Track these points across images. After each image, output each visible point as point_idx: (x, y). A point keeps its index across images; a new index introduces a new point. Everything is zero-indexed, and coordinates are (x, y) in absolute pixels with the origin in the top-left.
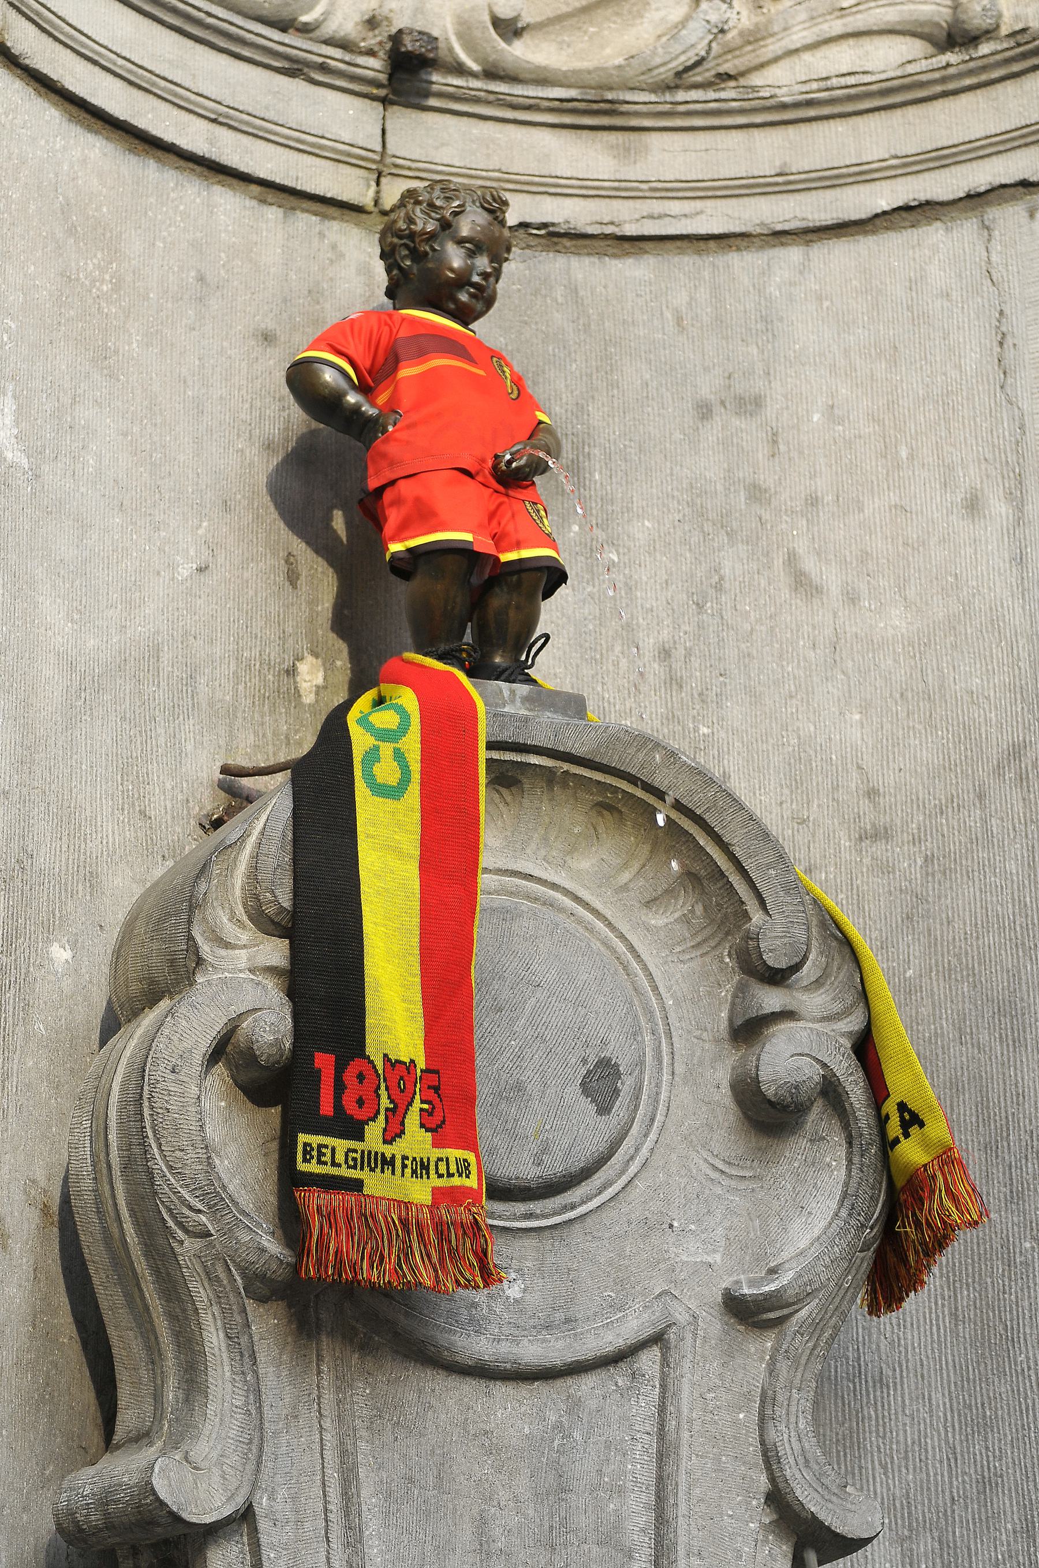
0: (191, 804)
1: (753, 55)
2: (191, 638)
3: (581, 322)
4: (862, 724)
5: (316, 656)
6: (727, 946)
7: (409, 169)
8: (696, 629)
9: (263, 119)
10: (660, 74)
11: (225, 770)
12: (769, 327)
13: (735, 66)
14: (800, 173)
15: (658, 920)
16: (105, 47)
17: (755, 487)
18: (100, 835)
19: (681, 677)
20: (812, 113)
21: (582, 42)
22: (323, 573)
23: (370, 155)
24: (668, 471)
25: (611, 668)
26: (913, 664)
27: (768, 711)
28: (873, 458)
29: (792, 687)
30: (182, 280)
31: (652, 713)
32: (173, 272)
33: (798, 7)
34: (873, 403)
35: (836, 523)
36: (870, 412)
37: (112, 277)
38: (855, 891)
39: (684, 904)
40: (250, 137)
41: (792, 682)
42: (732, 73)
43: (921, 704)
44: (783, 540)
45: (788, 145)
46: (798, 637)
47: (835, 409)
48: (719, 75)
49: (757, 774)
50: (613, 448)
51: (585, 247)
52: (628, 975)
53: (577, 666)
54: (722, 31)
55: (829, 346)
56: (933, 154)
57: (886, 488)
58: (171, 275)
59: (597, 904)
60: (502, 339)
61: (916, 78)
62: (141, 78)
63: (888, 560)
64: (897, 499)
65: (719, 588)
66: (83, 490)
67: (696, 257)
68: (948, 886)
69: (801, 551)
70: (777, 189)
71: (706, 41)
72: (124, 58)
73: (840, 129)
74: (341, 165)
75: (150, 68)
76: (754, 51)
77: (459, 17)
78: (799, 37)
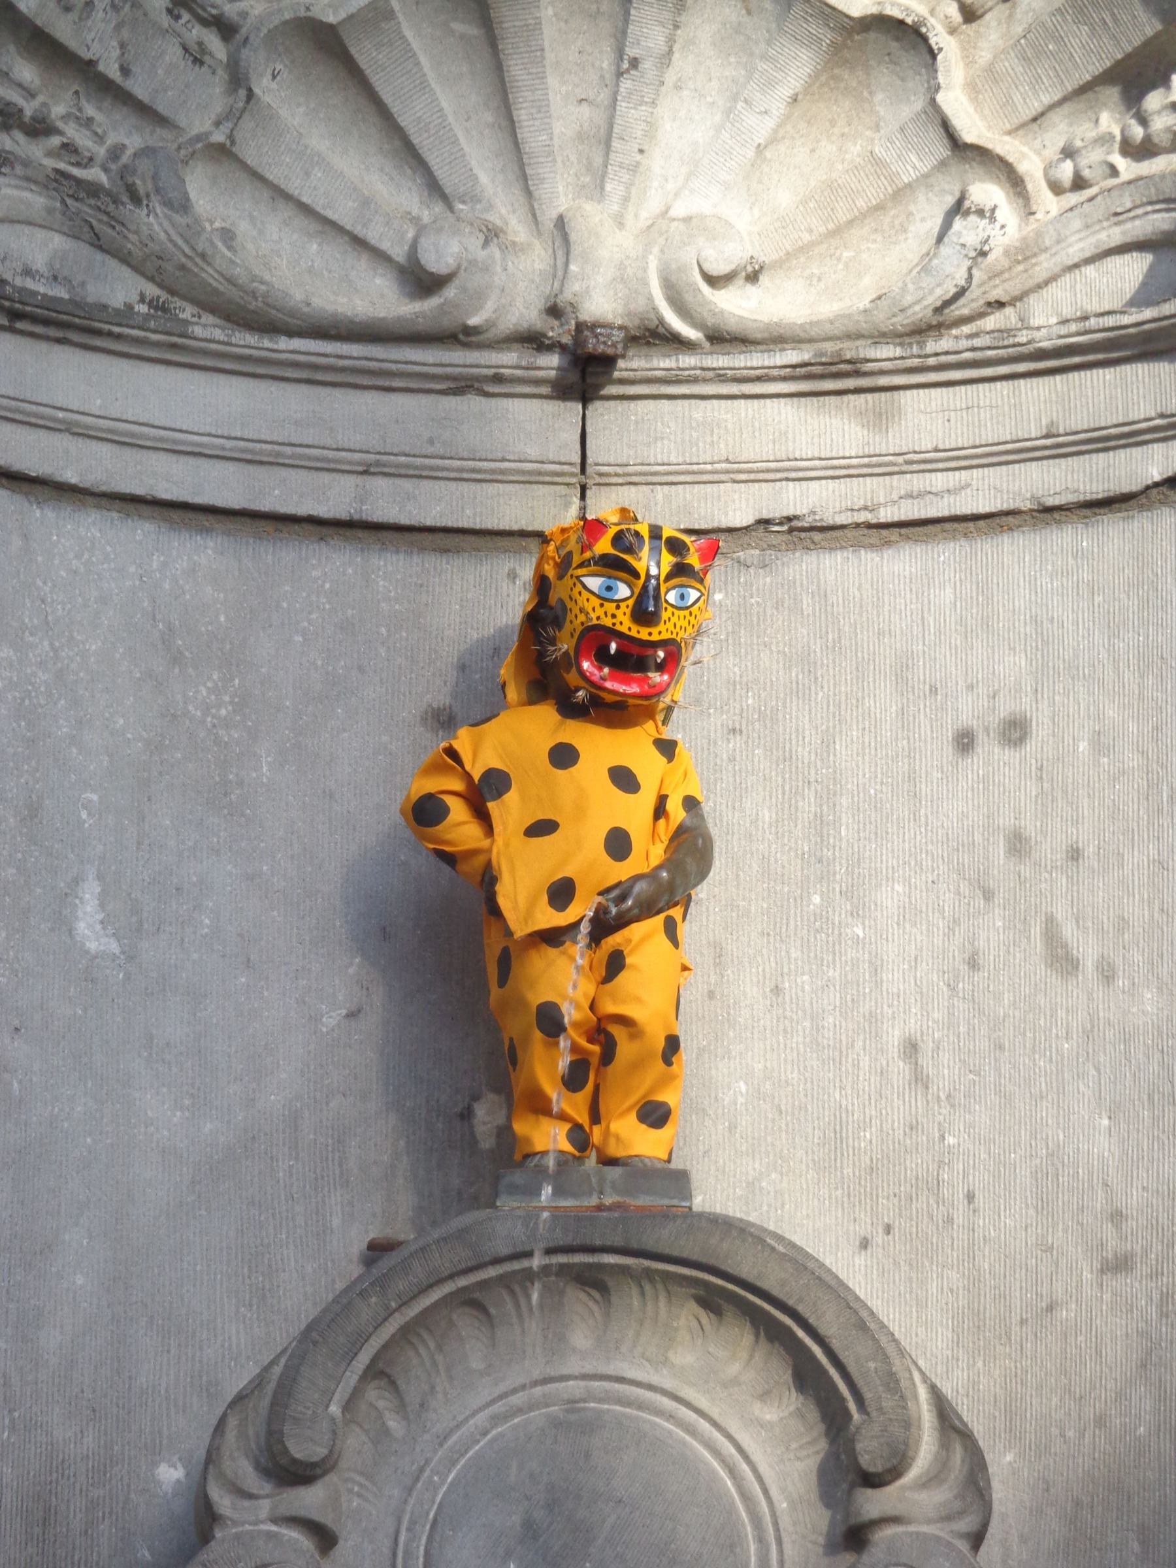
7: (617, 475)
9: (426, 457)
13: (1005, 291)
14: (1067, 434)
16: (209, 435)
18: (220, 1338)
19: (928, 1076)
23: (566, 468)
30: (327, 673)
33: (1069, 214)
40: (414, 480)
42: (1004, 300)
48: (989, 304)
54: (983, 254)
59: (703, 1403)
60: (736, 669)
62: (261, 452)
66: (195, 956)
76: (1026, 271)
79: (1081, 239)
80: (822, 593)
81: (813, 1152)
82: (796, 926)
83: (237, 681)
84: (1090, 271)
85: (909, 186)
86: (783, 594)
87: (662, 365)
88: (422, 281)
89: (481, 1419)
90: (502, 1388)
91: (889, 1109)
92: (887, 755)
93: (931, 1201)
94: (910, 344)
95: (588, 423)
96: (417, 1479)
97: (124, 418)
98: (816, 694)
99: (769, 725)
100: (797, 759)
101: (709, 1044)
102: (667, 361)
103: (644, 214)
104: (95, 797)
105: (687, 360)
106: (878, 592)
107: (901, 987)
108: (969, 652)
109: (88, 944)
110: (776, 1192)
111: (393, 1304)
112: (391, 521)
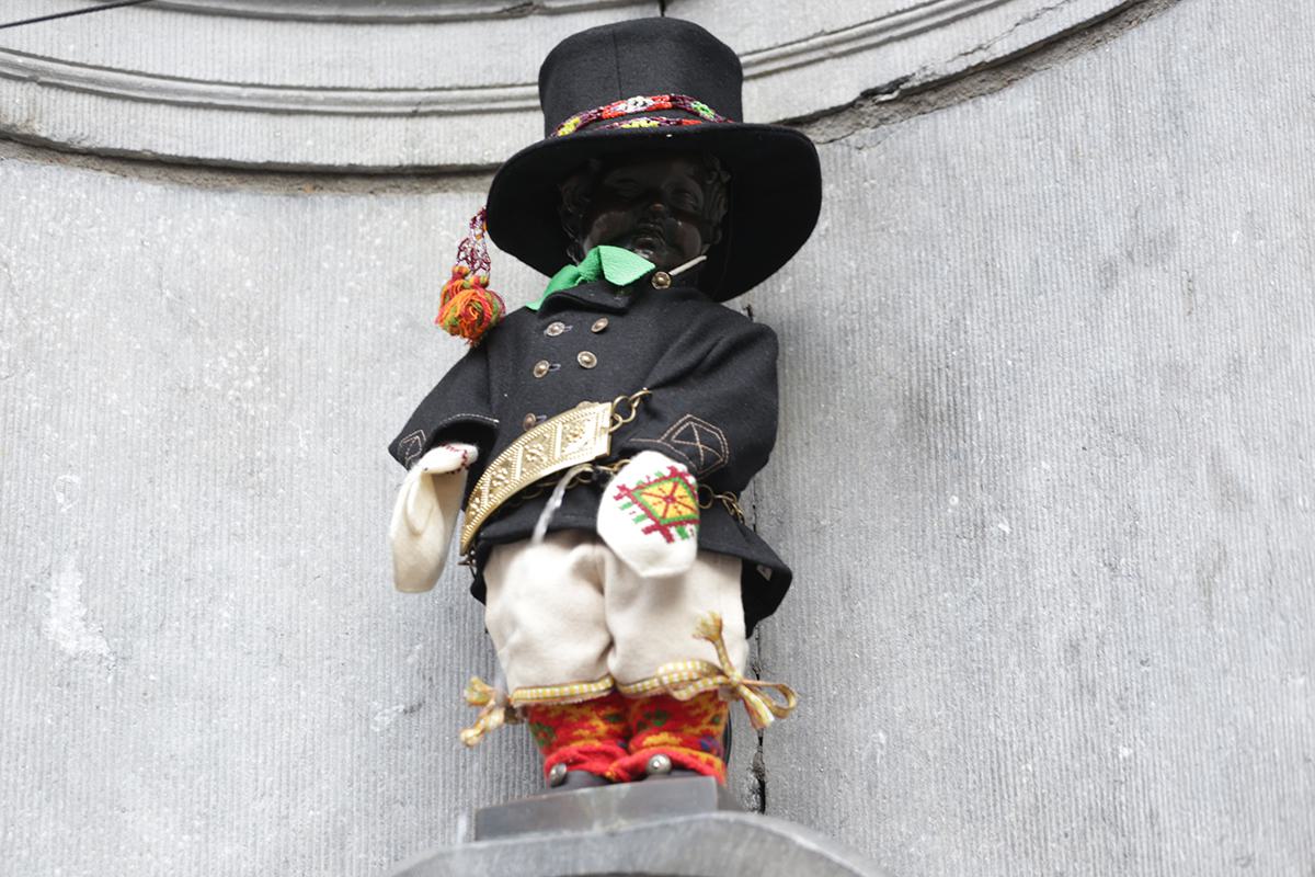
3: (953, 202)
4: (1306, 689)
9: (483, 87)
12: (1179, 123)
16: (220, 83)
24: (1068, 379)
29: (1226, 659)
31: (1058, 744)
32: (366, 330)
37: (262, 367)
40: (474, 117)
41: (1224, 649)
44: (1205, 436)
46: (1227, 578)
47: (1255, 215)
50: (998, 369)
51: (954, 94)
60: (852, 264)
62: (286, 99)
65: (1134, 533)
66: (209, 655)
69: (1226, 445)
72: (253, 85)
75: (294, 84)
80: (942, 156)
81: (968, 802)
82: (934, 536)
83: (266, 350)
86: (900, 168)
91: (1052, 731)
93: (1108, 835)
97: (107, 65)
98: (942, 269)
101: (840, 693)
104: (76, 479)
107: (1057, 582)
109: (63, 644)
110: (927, 856)
112: (449, 162)
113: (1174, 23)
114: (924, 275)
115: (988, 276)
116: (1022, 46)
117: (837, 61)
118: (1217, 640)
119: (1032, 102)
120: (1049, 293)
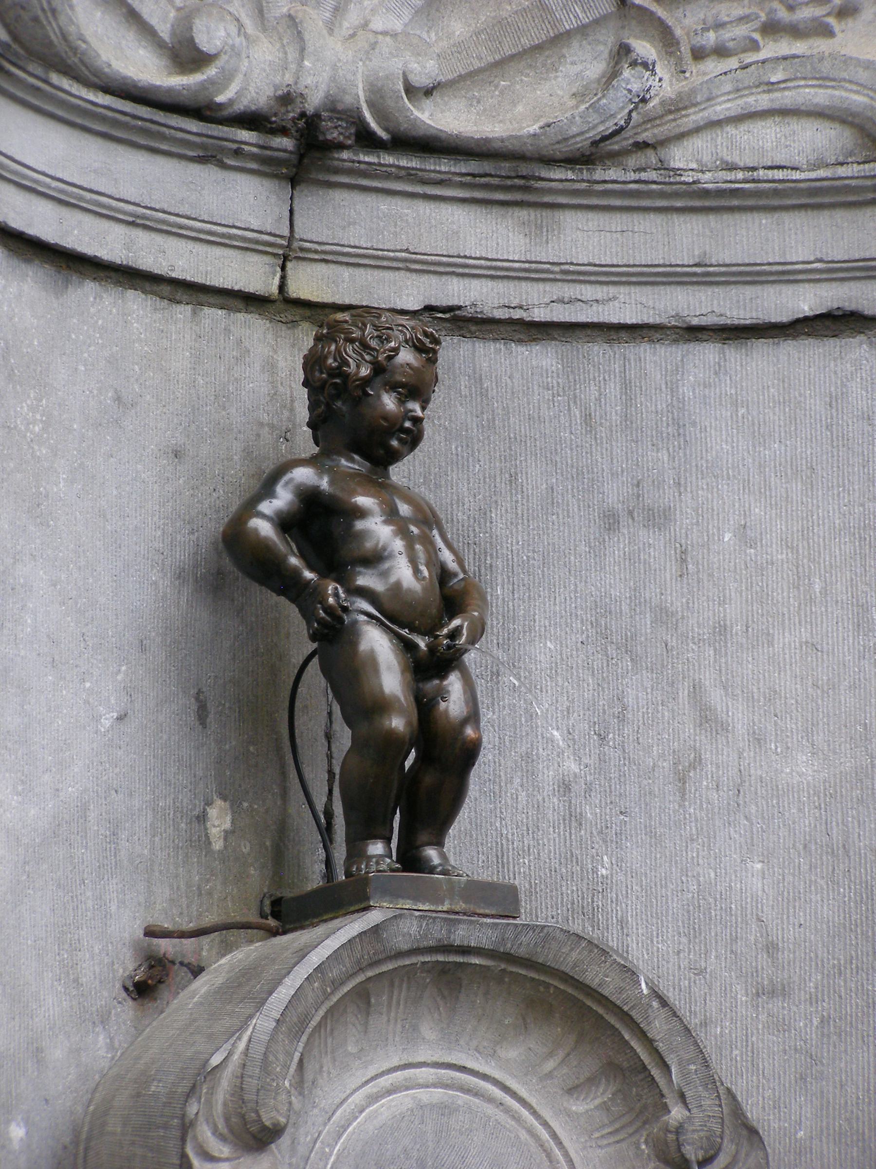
0: (115, 967)
1: (674, 124)
2: (113, 792)
4: (764, 873)
5: (224, 798)
6: (645, 1133)
8: (597, 762)
9: (177, 215)
10: (577, 143)
11: (150, 933)
12: (681, 431)
13: (655, 135)
14: (719, 265)
15: (579, 1107)
17: (661, 609)
20: (735, 202)
21: (492, 98)
22: (230, 708)
25: (509, 801)
26: (817, 815)
27: (668, 854)
28: (785, 588)
29: (694, 829)
30: (101, 402)
31: (550, 852)
32: (93, 397)
33: (723, 77)
34: (787, 527)
35: (745, 655)
36: (784, 537)
37: (42, 416)
38: (749, 1048)
39: (603, 1094)
40: (164, 235)
41: (693, 824)
43: (824, 858)
45: (708, 233)
46: (701, 776)
49: (654, 920)
50: (515, 560)
51: (491, 332)
52: (551, 1162)
53: (476, 799)
54: (644, 100)
55: (744, 459)
56: (861, 264)
57: (797, 622)
58: (91, 399)
59: (523, 1092)
61: (847, 182)
63: (797, 702)
64: (808, 635)
65: (622, 718)
66: (23, 653)
67: (606, 346)
68: (843, 1049)
69: (707, 683)
70: (695, 279)
71: (627, 111)
73: (764, 221)
74: (249, 253)
76: (675, 120)
77: (372, 84)
78: (722, 108)
79: (729, 100)
83: (44, 401)
84: (730, 130)
85: (568, 34)
87: (367, 159)
88: (187, 55)
89: (358, 1098)
90: (371, 1072)
91: (545, 840)
92: (538, 527)
94: (581, 170)
95: (296, 202)
96: (311, 1151)
98: (474, 466)
99: (433, 489)
100: (458, 522)
102: (371, 157)
103: (346, 24)
105: (388, 159)
106: (528, 382)
108: (614, 443)
111: (329, 989)
113: (683, 356)
114: (460, 466)
115: (511, 486)
116: (555, 320)
117: (408, 274)
118: (687, 816)
119: (554, 363)
120: (561, 516)
